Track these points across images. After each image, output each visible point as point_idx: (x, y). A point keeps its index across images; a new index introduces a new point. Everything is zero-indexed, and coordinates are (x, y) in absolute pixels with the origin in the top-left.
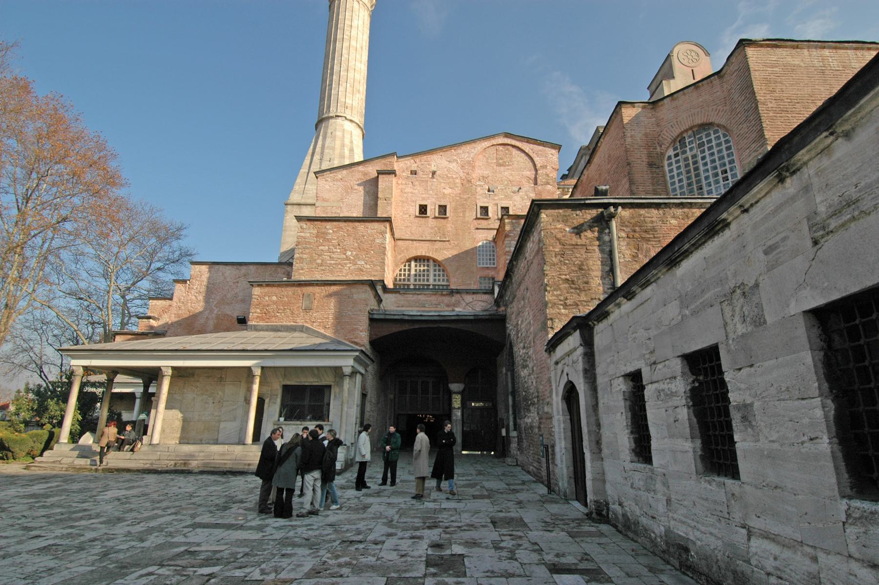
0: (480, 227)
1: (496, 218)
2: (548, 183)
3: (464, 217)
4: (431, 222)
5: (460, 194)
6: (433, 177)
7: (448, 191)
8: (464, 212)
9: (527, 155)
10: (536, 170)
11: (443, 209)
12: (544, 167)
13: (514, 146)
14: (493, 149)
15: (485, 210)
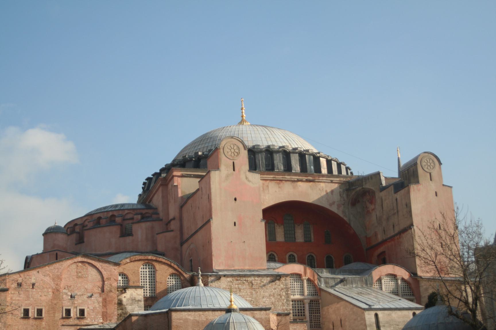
0: (64, 323)
1: (76, 317)
2: (111, 291)
3: (54, 317)
4: (31, 322)
5: (52, 300)
6: (33, 288)
7: (44, 298)
8: (54, 313)
9: (98, 269)
10: (103, 281)
11: (40, 312)
12: (109, 279)
13: (89, 263)
14: (74, 266)
15: (68, 312)
